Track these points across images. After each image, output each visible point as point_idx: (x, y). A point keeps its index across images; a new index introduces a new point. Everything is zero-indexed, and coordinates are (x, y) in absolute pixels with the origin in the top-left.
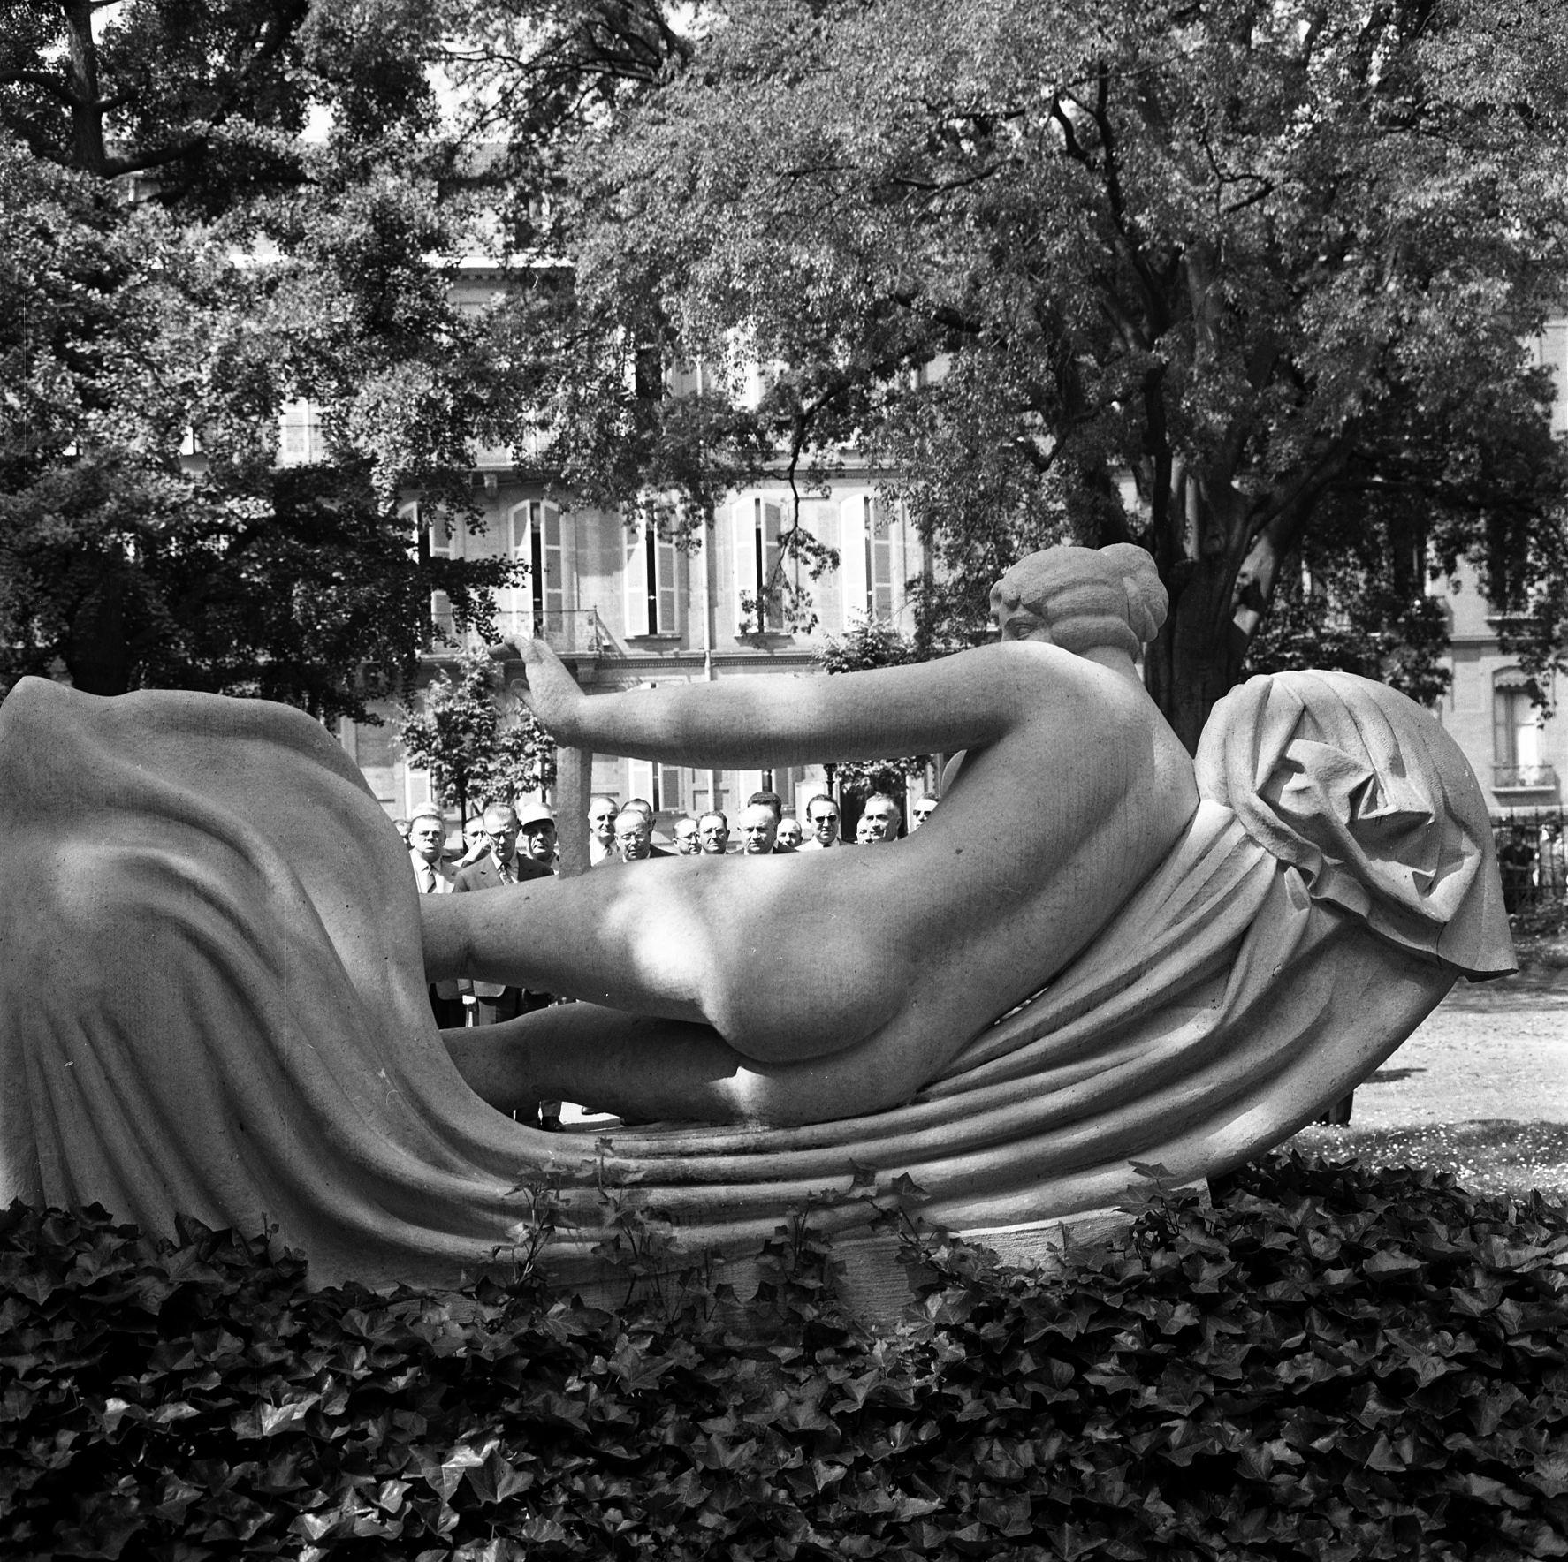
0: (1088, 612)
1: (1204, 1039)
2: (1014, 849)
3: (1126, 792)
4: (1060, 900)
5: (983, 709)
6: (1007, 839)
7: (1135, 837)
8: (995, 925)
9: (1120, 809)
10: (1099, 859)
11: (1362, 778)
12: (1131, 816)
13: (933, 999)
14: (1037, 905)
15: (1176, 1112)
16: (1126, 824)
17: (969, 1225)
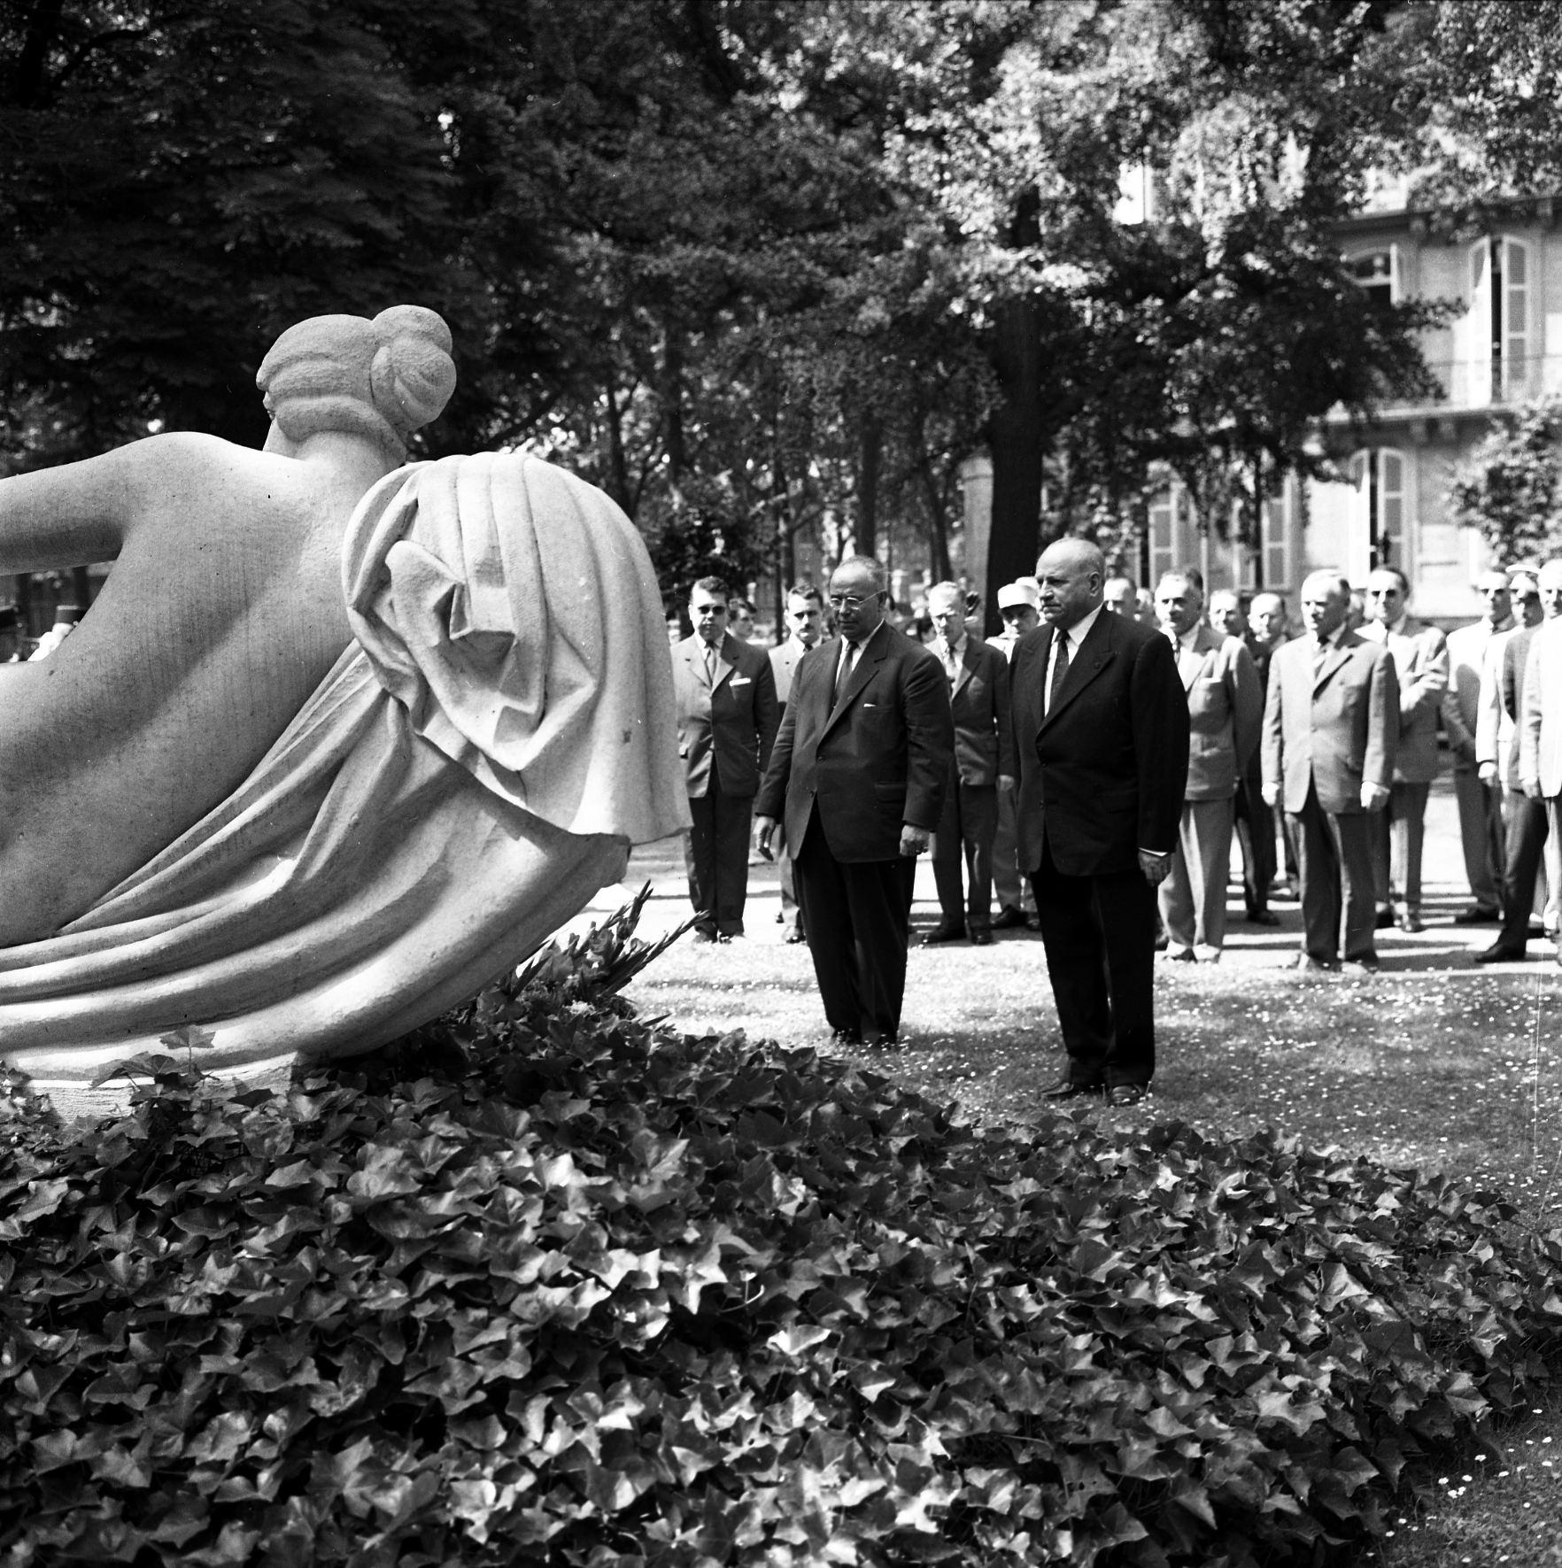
0: (300, 393)
1: (277, 895)
2: (100, 671)
3: (247, 604)
4: (174, 728)
5: (92, 512)
6: (92, 659)
7: (260, 658)
8: (103, 754)
9: (239, 626)
10: (215, 681)
11: (445, 589)
12: (253, 633)
13: (40, 832)
14: (148, 733)
15: (280, 967)
16: (249, 641)
17: (49, 1075)
